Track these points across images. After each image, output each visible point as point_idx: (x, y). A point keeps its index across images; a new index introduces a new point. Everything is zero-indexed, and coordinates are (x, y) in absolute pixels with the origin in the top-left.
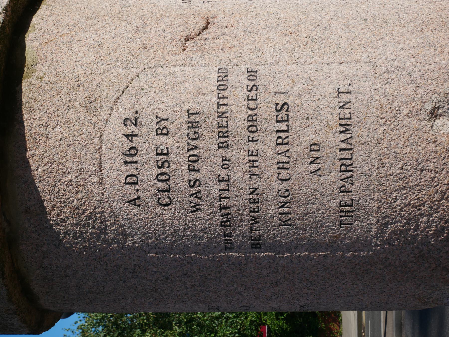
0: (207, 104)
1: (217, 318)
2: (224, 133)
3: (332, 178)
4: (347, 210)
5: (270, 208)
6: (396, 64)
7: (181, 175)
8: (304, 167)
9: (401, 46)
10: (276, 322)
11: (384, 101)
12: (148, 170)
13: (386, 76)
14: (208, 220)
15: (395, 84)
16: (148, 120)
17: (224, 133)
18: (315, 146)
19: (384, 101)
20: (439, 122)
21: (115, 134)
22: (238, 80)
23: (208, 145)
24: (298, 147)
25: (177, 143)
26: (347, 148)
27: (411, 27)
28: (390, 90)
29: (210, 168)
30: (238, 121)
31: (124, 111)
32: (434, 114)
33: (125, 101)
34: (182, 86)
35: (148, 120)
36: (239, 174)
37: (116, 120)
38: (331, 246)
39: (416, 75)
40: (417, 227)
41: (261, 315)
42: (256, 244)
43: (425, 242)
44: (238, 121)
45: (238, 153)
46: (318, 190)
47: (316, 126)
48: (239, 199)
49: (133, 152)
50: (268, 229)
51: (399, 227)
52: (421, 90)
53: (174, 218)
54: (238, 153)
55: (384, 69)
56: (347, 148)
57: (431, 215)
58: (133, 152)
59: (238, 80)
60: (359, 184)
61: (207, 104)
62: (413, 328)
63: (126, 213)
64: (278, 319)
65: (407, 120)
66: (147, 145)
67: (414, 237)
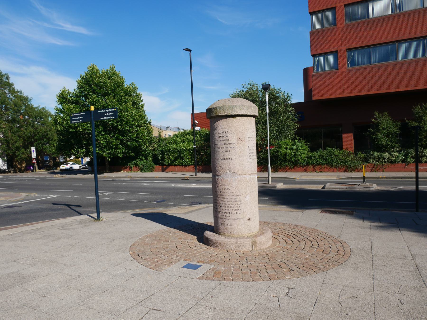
0: (230, 142)
1: (273, 132)
2: (226, 144)
3: (221, 158)
4: (218, 160)
5: (218, 150)
7: (221, 139)
8: (222, 154)
12: (221, 135)
14: (217, 142)
16: (227, 135)
17: (226, 144)
18: (225, 155)
21: (226, 130)
22: (233, 146)
23: (225, 142)
24: (225, 153)
25: (225, 138)
26: (225, 159)
29: (222, 143)
30: (227, 146)
31: (229, 131)
33: (230, 131)
34: (232, 138)
35: (227, 135)
36: (222, 146)
37: (228, 130)
38: (215, 158)
42: (215, 148)
44: (227, 146)
45: (224, 146)
46: (220, 156)
47: (227, 156)
48: (219, 146)
49: (224, 133)
50: (216, 150)
53: (217, 138)
54: (224, 146)
56: (225, 159)
58: (224, 133)
59: (233, 146)
60: (221, 161)
61: (230, 142)
63: (217, 132)
66: (224, 134)
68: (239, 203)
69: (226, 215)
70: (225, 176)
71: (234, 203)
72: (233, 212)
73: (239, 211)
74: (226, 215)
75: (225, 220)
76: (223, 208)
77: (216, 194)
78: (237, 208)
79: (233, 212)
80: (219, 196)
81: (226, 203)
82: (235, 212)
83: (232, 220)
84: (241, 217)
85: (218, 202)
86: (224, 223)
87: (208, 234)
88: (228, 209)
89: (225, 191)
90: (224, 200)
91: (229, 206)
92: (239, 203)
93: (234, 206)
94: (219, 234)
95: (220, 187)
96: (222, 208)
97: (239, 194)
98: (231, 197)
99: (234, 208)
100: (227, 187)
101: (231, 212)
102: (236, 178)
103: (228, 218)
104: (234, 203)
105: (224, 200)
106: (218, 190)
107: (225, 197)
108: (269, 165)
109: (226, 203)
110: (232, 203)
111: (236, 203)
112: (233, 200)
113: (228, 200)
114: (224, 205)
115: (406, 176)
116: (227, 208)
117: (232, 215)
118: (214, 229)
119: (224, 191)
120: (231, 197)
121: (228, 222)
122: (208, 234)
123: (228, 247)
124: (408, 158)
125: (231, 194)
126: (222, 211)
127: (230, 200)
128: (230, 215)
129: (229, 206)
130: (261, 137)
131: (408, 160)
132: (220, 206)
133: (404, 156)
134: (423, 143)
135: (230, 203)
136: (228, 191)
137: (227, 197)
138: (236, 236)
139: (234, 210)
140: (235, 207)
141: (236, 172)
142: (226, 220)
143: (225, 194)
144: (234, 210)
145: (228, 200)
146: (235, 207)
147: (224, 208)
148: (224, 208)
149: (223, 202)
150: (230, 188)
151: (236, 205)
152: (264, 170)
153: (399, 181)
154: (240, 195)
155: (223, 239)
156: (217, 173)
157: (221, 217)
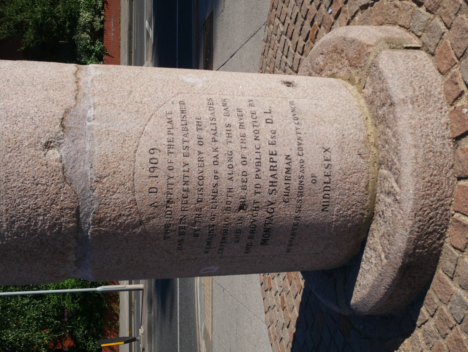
1: (27, 304)
6: (23, 111)
9: (29, 99)
10: (72, 305)
11: (11, 136)
13: (15, 119)
15: (20, 125)
19: (11, 136)
20: (51, 152)
27: (39, 87)
28: (16, 128)
32: (47, 146)
39: (36, 119)
40: (36, 223)
41: (61, 300)
43: (43, 233)
51: (23, 223)
52: (38, 130)
55: (14, 114)
57: (45, 215)
62: (158, 303)
64: (73, 303)
65: (27, 150)
67: (35, 231)
68: (219, 108)
69: (281, 175)
70: (86, 170)
71: (222, 130)
72: (266, 136)
73: (259, 111)
74: (281, 175)
75: (307, 182)
76: (251, 188)
77: (182, 232)
78: (248, 121)
79: (266, 136)
80: (191, 215)
81: (223, 170)
82: (264, 128)
83: (306, 145)
84: (287, 108)
85: (219, 221)
86: (320, 186)
87: (371, 278)
88: (252, 160)
89: (161, 172)
90: (209, 182)
91: (237, 158)
92: (219, 108)
93: (236, 133)
94: (370, 219)
95: (144, 200)
96: (251, 197)
97: (177, 108)
98: (193, 143)
99: (249, 131)
100: (143, 159)
101: (266, 149)
102: (91, 113)
103: (295, 165)
104: (222, 130)
105: (209, 182)
106: (159, 222)
107: (195, 174)
108: (99, 289)
109: (223, 170)
110: (222, 138)
111: (221, 121)
112: (206, 135)
113: (209, 160)
114: (236, 184)
115: (126, 46)
116: (251, 169)
117: (279, 141)
118: (329, 279)
119: (162, 182)
120: (193, 143)
121: (314, 165)
122: (371, 278)
123: (438, 142)
124: (93, 50)
125: (178, 143)
126: (265, 197)
127: (207, 148)
128: (282, 151)
129: (237, 158)
130: (36, 331)
131: (98, 49)
132: (242, 207)
133: (90, 56)
134: (67, 25)
135: (223, 149)
136: (162, 158)
137: (193, 161)
138: (371, 129)
139: (257, 132)
140: (241, 126)
141: (59, 112)
142: (308, 174)
143: (178, 174)
144: (257, 132)
145: (209, 160)
146: (241, 126)
147: (252, 181)
148: (252, 181)
149: (223, 188)
150: (145, 145)
151: (234, 120)
152: (114, 324)
153: (135, 51)
154: (182, 103)
155: (407, 169)
156: (67, 222)
157: (293, 202)
